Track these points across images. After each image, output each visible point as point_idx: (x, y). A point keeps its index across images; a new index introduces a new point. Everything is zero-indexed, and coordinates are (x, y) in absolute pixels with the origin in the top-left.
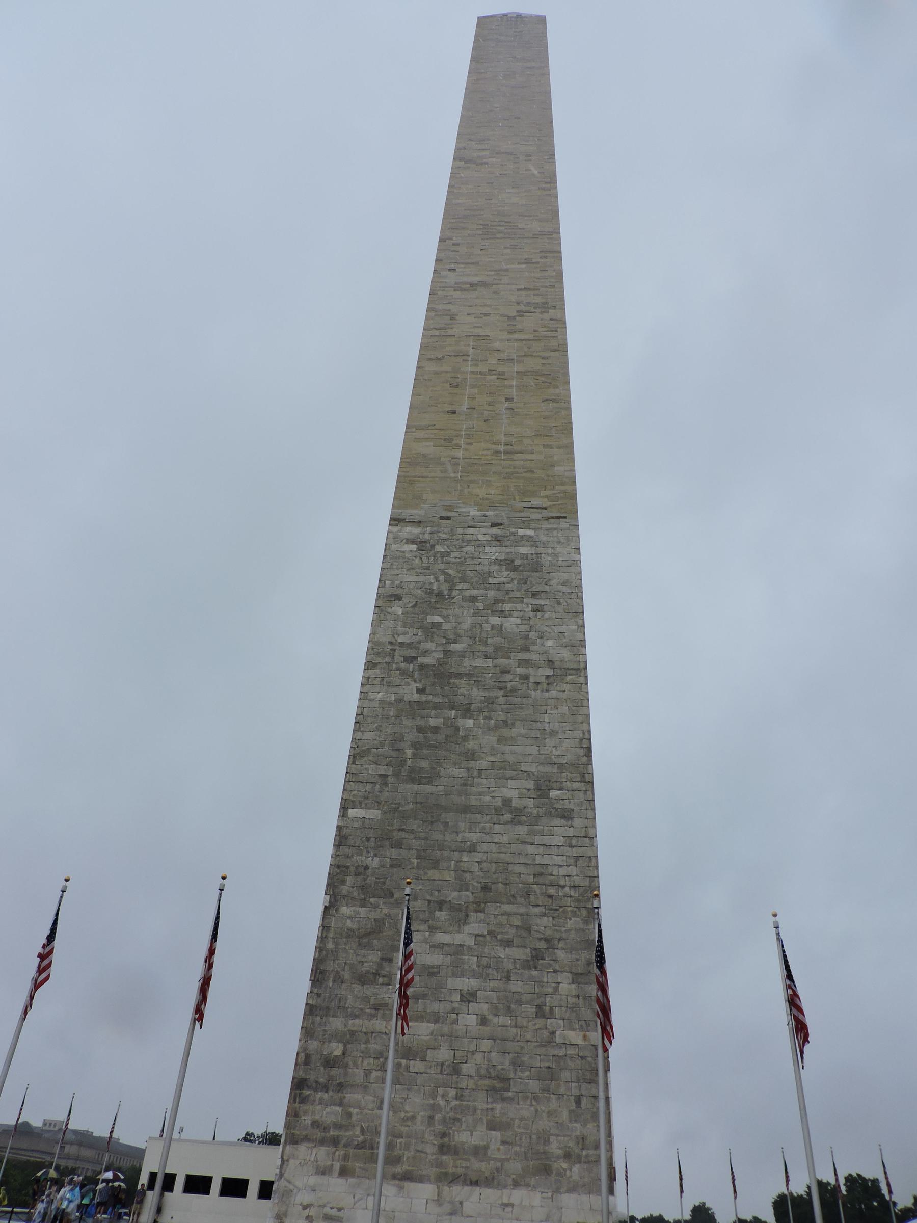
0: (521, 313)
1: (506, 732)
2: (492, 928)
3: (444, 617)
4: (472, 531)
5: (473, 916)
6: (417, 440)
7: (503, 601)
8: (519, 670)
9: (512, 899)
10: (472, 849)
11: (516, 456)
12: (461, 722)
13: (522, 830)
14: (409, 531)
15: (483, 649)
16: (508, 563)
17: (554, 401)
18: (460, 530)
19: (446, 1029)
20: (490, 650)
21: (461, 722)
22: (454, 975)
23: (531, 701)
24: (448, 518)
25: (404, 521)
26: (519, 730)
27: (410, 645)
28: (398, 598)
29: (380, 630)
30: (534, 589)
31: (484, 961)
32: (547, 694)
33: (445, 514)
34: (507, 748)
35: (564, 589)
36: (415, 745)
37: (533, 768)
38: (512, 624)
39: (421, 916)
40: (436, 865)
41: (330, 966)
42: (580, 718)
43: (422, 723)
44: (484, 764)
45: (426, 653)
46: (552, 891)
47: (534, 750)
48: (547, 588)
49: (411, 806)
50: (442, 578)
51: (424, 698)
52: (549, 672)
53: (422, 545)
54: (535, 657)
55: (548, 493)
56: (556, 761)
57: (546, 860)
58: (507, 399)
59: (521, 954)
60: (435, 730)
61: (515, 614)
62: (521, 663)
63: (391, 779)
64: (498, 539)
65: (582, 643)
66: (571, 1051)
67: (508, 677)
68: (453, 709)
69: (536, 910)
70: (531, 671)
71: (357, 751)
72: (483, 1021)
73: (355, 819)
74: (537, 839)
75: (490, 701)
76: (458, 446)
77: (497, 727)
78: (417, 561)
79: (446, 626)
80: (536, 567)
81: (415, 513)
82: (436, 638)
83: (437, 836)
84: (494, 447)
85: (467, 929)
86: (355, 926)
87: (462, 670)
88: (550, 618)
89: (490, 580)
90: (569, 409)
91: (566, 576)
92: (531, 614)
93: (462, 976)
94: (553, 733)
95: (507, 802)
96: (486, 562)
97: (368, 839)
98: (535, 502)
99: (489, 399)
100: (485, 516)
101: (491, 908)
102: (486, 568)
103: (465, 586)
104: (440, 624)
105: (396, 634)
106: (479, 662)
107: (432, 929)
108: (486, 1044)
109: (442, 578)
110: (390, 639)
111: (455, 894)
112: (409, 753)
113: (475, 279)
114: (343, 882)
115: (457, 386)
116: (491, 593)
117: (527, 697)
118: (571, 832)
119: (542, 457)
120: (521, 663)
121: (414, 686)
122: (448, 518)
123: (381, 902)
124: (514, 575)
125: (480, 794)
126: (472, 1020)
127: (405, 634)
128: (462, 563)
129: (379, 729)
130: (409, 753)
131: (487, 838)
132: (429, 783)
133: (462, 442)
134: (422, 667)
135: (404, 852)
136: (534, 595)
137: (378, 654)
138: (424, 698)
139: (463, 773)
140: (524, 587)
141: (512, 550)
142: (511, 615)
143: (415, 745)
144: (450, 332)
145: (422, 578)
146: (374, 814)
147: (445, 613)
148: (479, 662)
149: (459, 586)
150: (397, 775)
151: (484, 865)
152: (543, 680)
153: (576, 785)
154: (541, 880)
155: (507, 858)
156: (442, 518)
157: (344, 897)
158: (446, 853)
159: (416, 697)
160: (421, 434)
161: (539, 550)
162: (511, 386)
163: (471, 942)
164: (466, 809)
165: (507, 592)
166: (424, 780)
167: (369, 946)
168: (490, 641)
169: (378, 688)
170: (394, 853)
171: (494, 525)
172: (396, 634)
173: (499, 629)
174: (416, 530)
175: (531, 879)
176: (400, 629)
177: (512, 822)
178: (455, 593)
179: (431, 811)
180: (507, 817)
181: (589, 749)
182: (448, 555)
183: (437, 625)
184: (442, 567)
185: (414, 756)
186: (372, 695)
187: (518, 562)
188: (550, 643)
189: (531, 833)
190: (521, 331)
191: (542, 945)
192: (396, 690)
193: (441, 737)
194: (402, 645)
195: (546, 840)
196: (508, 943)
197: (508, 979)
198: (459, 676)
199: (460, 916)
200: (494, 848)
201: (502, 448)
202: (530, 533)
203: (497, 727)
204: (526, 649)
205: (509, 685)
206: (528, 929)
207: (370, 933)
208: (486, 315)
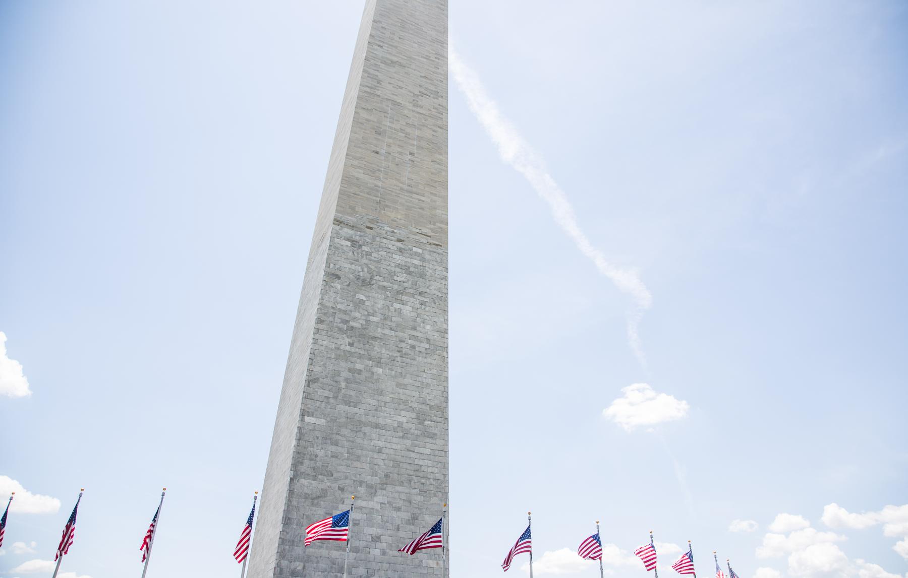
0: (422, 94)
1: (401, 380)
2: (390, 500)
3: (366, 296)
4: (384, 241)
5: (379, 492)
6: (353, 166)
7: (402, 294)
8: (410, 342)
9: (401, 484)
10: (380, 452)
11: (415, 196)
12: (375, 369)
13: (408, 443)
15: (389, 323)
16: (407, 269)
17: (439, 164)
18: (378, 239)
19: (363, 557)
20: (394, 325)
21: (375, 369)
22: (368, 526)
23: (415, 363)
24: (371, 228)
25: (343, 223)
26: (408, 380)
27: (345, 312)
28: (338, 277)
29: (326, 297)
30: (421, 290)
31: (385, 518)
32: (425, 360)
33: (369, 225)
34: (401, 391)
35: (438, 293)
36: (347, 380)
37: (415, 405)
38: (407, 310)
39: (350, 489)
40: (358, 459)
41: (294, 515)
42: (442, 378)
43: (351, 366)
44: (388, 399)
46: (423, 481)
47: (416, 394)
48: (428, 291)
49: (343, 420)
50: (366, 269)
51: (353, 349)
52: (427, 346)
53: (354, 243)
54: (419, 334)
55: (432, 226)
56: (428, 402)
57: (421, 462)
58: (410, 153)
59: (405, 515)
60: (359, 372)
61: (409, 304)
62: (412, 337)
63: (332, 401)
64: (401, 250)
65: (446, 332)
66: (430, 571)
67: (403, 345)
68: (370, 360)
69: (414, 491)
70: (416, 343)
71: (311, 378)
72: (384, 553)
73: (309, 424)
74: (417, 450)
76: (379, 178)
77: (395, 377)
78: (351, 253)
79: (367, 303)
80: (422, 275)
81: (351, 220)
82: (361, 310)
83: (359, 441)
84: (401, 185)
85: (376, 499)
86: (309, 492)
87: (377, 335)
88: (429, 311)
89: (395, 278)
90: (447, 171)
91: (439, 285)
92: (419, 306)
93: (373, 526)
94: (428, 385)
95: (400, 424)
96: (393, 265)
97: (318, 438)
98: (424, 230)
99: (399, 150)
100: (393, 232)
101: (389, 488)
102: (393, 269)
103: (380, 278)
104: (364, 301)
105: (336, 302)
106: (387, 332)
107: (355, 498)
108: (386, 566)
109: (366, 269)
110: (331, 304)
111: (369, 477)
112: (343, 385)
113: (395, 59)
114: (302, 463)
115: (380, 134)
116: (396, 287)
117: (414, 359)
118: (435, 447)
119: (429, 200)
120: (412, 337)
121: (347, 340)
122: (371, 228)
123: (325, 478)
124: (409, 277)
125: (385, 417)
126: (377, 552)
127: (342, 303)
128: (379, 262)
129: (324, 365)
130: (343, 385)
131: (388, 445)
132: (355, 406)
133: (382, 175)
134: (352, 328)
135: (340, 449)
136: (421, 294)
137: (325, 314)
138: (353, 349)
139: (375, 403)
140: (415, 287)
141: (409, 260)
142: (406, 304)
143: (347, 380)
144: (377, 93)
145: (353, 267)
146: (322, 422)
147: (367, 294)
148: (387, 332)
149: (377, 278)
150: (336, 398)
151: (386, 462)
152: (423, 350)
153: (439, 419)
154: (417, 473)
155: (399, 458)
156: (367, 227)
157: (302, 473)
158: (364, 452)
159: (348, 348)
160: (356, 163)
161: (424, 264)
162: (413, 145)
163: (378, 507)
164: (377, 426)
165: (405, 288)
166: (352, 404)
167: (318, 505)
168: (393, 319)
169: (324, 338)
170: (333, 448)
171: (399, 240)
172: (336, 302)
173: (399, 312)
175: (412, 473)
176: (339, 300)
177: (403, 437)
178: (373, 282)
179: (357, 425)
180: (401, 434)
181: (447, 398)
182: (370, 255)
183: (361, 302)
184: (367, 262)
185: (347, 387)
186: (320, 342)
187: (412, 269)
188: (428, 327)
189: (414, 445)
190: (421, 107)
191: (417, 511)
192: (335, 341)
193: (362, 377)
194: (340, 310)
195: (421, 450)
196: (398, 509)
197: (398, 529)
198: (375, 338)
199: (372, 491)
200: (392, 452)
201: (406, 187)
202: (420, 251)
203: (395, 377)
204: (414, 329)
205: (404, 350)
206: (410, 502)
207: (319, 497)
208: (401, 88)
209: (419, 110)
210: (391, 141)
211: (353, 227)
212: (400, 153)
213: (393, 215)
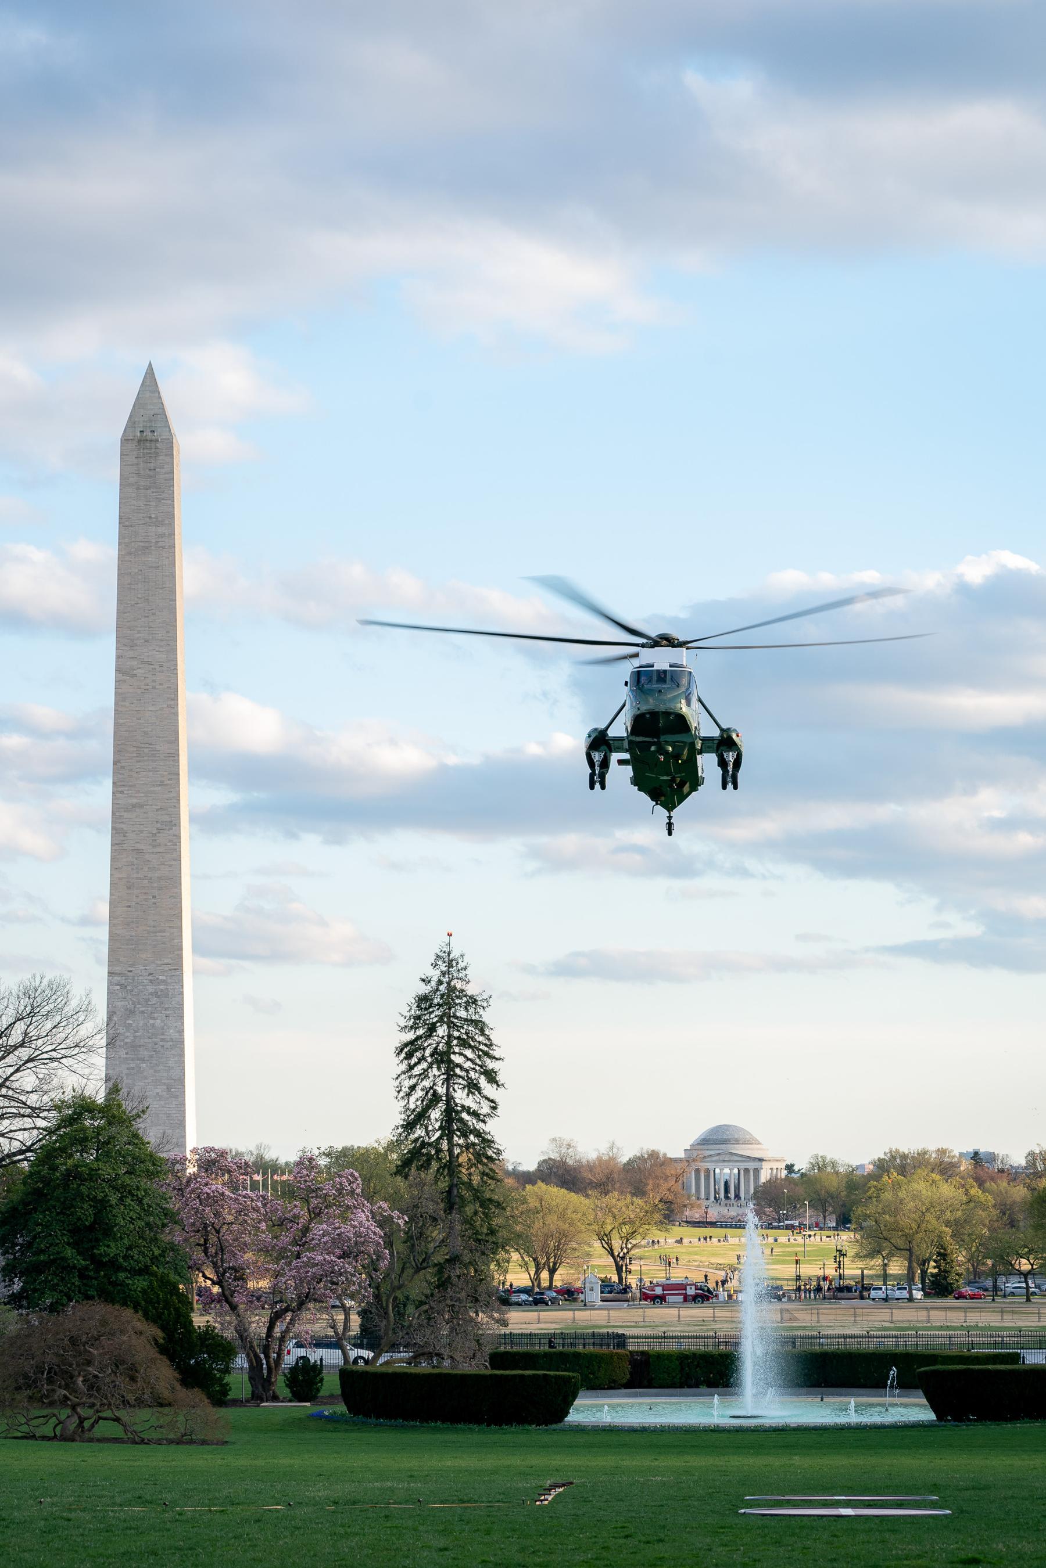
13: (162, 1103)
26: (161, 1067)
60: (133, 1068)
75: (151, 1056)
80: (167, 996)
81: (118, 969)
113: (135, 801)
134: (126, 1043)
171: (150, 974)
174: (119, 978)
208: (142, 832)
209: (158, 850)
212: (146, 900)
213: (144, 956)
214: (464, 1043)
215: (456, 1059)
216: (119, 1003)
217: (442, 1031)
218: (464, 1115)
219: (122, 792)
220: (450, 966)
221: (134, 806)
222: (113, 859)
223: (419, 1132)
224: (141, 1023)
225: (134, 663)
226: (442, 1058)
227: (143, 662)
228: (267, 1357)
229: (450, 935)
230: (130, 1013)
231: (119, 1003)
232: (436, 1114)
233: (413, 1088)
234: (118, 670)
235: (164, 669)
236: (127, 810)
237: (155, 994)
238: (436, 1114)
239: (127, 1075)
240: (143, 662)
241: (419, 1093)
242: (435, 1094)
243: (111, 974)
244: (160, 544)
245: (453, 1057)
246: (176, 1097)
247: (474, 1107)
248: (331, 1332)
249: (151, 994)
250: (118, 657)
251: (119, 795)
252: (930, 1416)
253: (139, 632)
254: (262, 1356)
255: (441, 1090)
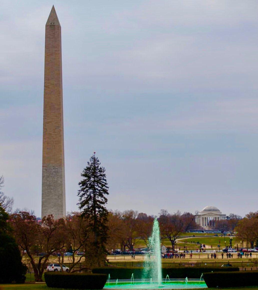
14: (45, 168)
36: (48, 193)
45: (47, 183)
60: (49, 191)
80: (58, 172)
81: (45, 165)
113: (49, 121)
134: (47, 185)
171: (53, 167)
198: (51, 185)
204: (57, 182)
208: (51, 129)
209: (55, 134)
210: (50, 144)
211: (46, 167)
214: (97, 182)
215: (97, 187)
216: (45, 174)
217: (92, 179)
218: (98, 203)
219: (46, 118)
220: (95, 160)
221: (49, 122)
222: (43, 136)
223: (86, 207)
224: (51, 179)
225: (49, 84)
226: (92, 187)
227: (51, 84)
228: (39, 270)
229: (95, 153)
230: (48, 177)
231: (45, 174)
232: (91, 202)
233: (84, 194)
234: (45, 86)
235: (57, 86)
236: (47, 123)
237: (55, 172)
238: (91, 202)
239: (48, 193)
240: (51, 84)
241: (86, 196)
242: (91, 196)
243: (43, 166)
244: (56, 53)
245: (95, 187)
246: (60, 199)
247: (101, 200)
248: (58, 262)
249: (54, 172)
250: (45, 83)
251: (45, 119)
252: (206, 287)
253: (50, 76)
254: (38, 269)
255: (92, 195)
